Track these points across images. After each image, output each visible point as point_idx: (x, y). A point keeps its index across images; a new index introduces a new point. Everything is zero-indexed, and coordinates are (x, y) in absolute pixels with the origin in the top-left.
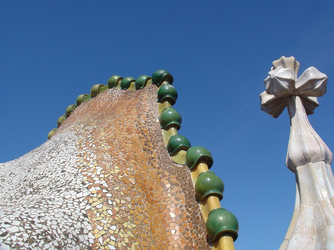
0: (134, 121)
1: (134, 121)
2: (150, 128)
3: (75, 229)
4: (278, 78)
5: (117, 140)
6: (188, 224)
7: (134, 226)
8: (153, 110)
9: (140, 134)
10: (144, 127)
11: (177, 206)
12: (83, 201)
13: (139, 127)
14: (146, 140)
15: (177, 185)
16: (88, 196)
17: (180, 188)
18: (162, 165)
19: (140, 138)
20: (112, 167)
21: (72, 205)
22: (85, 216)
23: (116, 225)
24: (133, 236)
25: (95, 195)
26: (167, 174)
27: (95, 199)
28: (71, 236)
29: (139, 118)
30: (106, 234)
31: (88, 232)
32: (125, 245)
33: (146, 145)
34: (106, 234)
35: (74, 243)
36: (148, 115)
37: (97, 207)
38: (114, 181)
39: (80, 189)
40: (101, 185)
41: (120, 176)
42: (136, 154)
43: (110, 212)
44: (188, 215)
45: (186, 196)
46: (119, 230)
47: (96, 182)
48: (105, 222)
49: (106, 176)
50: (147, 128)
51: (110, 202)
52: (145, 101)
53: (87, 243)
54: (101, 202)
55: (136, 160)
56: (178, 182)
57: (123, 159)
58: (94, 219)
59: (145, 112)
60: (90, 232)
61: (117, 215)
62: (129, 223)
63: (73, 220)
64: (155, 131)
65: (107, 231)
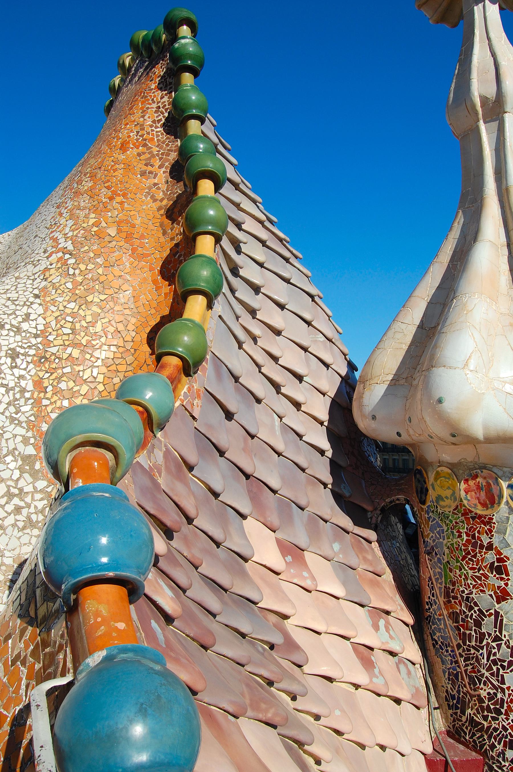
0: (135, 125)
1: (135, 125)
3: (17, 317)
5: (103, 168)
7: (103, 297)
9: (141, 148)
10: (148, 133)
12: (39, 277)
13: (140, 136)
14: (149, 156)
16: (46, 268)
19: (139, 155)
20: (87, 217)
21: (24, 285)
22: (37, 296)
23: (75, 301)
24: (99, 311)
25: (54, 266)
27: (52, 271)
28: (7, 327)
29: (143, 117)
30: (61, 315)
31: (37, 316)
32: (85, 325)
33: (146, 165)
34: (61, 315)
35: (12, 334)
36: (159, 107)
37: (54, 281)
38: (83, 239)
39: (39, 260)
40: (65, 248)
41: (95, 229)
42: (127, 186)
43: (70, 285)
46: (80, 306)
47: (60, 246)
48: (60, 299)
49: (75, 233)
50: (155, 132)
51: (71, 271)
53: (34, 331)
54: (59, 274)
55: (124, 195)
57: (104, 200)
58: (48, 299)
59: (154, 102)
60: (40, 317)
61: (79, 287)
62: (96, 294)
63: (17, 305)
65: (62, 310)
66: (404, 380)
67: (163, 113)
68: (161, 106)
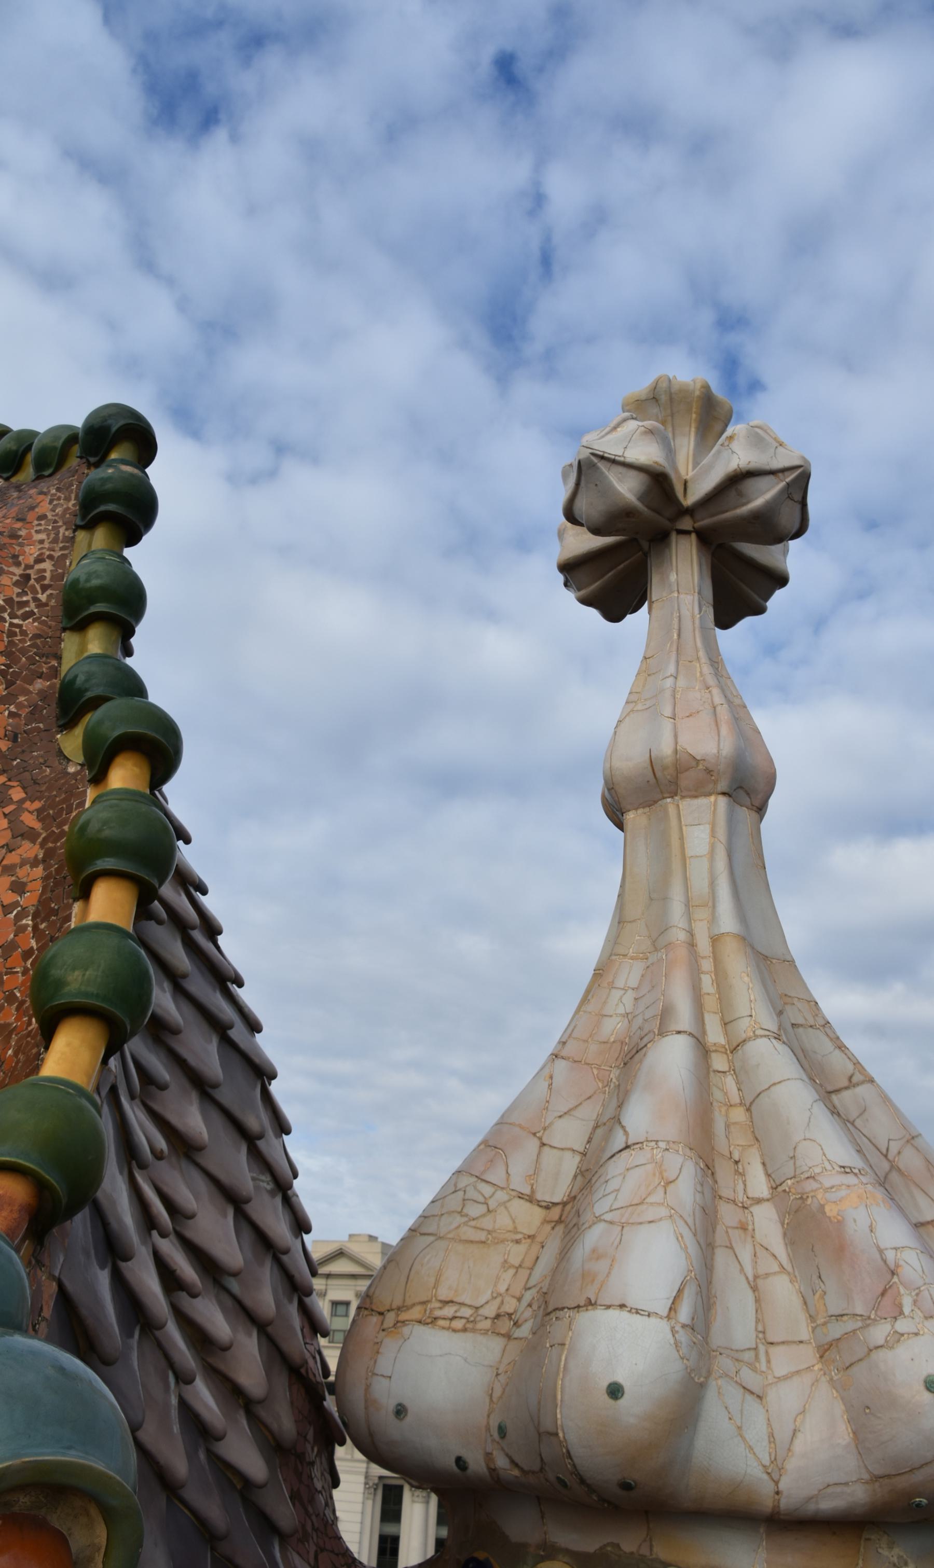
2: (20, 626)
4: (602, 458)
6: (21, 978)
8: (51, 557)
11: (12, 912)
15: (30, 835)
17: (37, 846)
18: (15, 763)
26: (17, 794)
44: (32, 947)
45: (45, 879)
50: (7, 625)
52: (36, 522)
56: (37, 826)
59: (18, 564)
64: (36, 636)
66: (489, 1322)
67: (34, 591)
68: (33, 576)
